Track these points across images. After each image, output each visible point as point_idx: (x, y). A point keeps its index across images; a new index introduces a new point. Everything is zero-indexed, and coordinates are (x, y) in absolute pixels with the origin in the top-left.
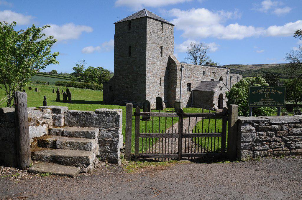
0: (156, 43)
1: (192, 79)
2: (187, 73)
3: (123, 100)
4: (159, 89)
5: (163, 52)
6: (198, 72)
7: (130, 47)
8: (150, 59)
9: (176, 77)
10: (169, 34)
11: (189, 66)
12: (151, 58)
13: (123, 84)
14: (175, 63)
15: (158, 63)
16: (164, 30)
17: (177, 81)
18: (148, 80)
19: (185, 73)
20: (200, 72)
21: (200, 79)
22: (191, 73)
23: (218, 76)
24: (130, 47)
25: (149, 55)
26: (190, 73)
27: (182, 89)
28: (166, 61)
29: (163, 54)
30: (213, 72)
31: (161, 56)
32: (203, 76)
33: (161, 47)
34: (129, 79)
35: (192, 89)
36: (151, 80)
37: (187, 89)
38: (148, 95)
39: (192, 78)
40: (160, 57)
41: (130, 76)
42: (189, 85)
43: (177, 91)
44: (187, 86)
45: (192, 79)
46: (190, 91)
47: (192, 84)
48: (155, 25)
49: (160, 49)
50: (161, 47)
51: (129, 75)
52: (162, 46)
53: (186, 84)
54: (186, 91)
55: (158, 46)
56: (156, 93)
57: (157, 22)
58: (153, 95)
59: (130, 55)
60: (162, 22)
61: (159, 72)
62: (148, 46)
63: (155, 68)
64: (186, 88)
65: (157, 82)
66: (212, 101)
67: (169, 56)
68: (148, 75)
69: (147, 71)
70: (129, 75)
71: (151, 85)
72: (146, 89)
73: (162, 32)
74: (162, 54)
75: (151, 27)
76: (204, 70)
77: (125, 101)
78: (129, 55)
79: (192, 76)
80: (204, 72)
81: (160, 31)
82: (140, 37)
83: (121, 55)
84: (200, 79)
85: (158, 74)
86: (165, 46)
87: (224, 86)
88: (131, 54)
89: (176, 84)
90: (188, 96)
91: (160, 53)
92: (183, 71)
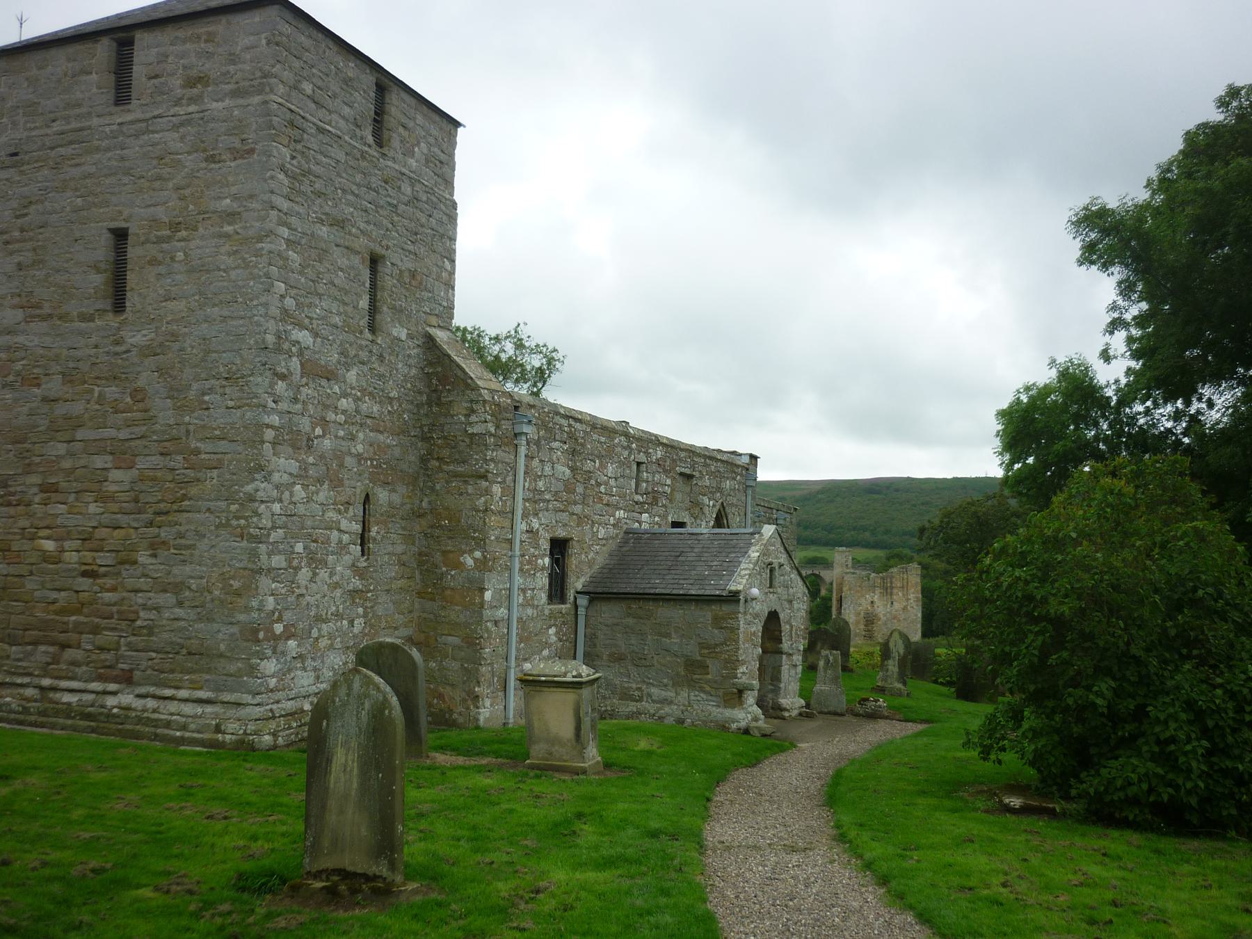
0: (339, 223)
1: (577, 509)
2: (548, 470)
3: (46, 682)
4: (357, 583)
5: (382, 295)
6: (611, 469)
7: (120, 235)
8: (304, 337)
9: (487, 492)
10: (428, 178)
11: (557, 419)
12: (302, 327)
13: (49, 545)
14: (476, 388)
15: (352, 375)
16: (396, 143)
17: (493, 520)
18: (276, 507)
19: (536, 463)
20: (621, 464)
21: (620, 514)
22: (573, 469)
23: (706, 500)
24: (120, 235)
25: (289, 303)
26: (564, 471)
27: (518, 580)
28: (405, 368)
29: (385, 315)
30: (681, 474)
31: (373, 328)
32: (638, 498)
33: (375, 262)
34: (103, 498)
35: (577, 582)
36: (301, 509)
37: (546, 581)
38: (279, 628)
39: (575, 503)
40: (368, 335)
41: (115, 475)
42: (559, 547)
43: (488, 595)
44: (547, 560)
45: (577, 509)
46: (563, 600)
47: (574, 549)
48: (335, 87)
49: (366, 274)
50: (375, 262)
51: (99, 462)
52: (380, 251)
53: (546, 546)
54: (543, 597)
55: (356, 246)
56: (338, 616)
57: (351, 69)
58: (315, 633)
59: (119, 305)
60: (385, 84)
61: (360, 448)
62: (285, 232)
63: (331, 416)
64: (543, 580)
65: (344, 524)
66: (732, 664)
67: (430, 339)
68: (284, 464)
69: (269, 434)
70: (99, 462)
71: (299, 547)
72: (265, 583)
73: (385, 150)
74: (373, 309)
75: (308, 88)
76: (642, 457)
77: (64, 684)
78: (110, 301)
79: (580, 489)
80: (639, 464)
81: (370, 139)
82: (211, 159)
83: (38, 306)
84: (620, 514)
85: (349, 461)
86: (397, 261)
87: (783, 558)
88: (132, 299)
89: (481, 543)
90: (552, 631)
91: (364, 303)
92: (523, 450)
